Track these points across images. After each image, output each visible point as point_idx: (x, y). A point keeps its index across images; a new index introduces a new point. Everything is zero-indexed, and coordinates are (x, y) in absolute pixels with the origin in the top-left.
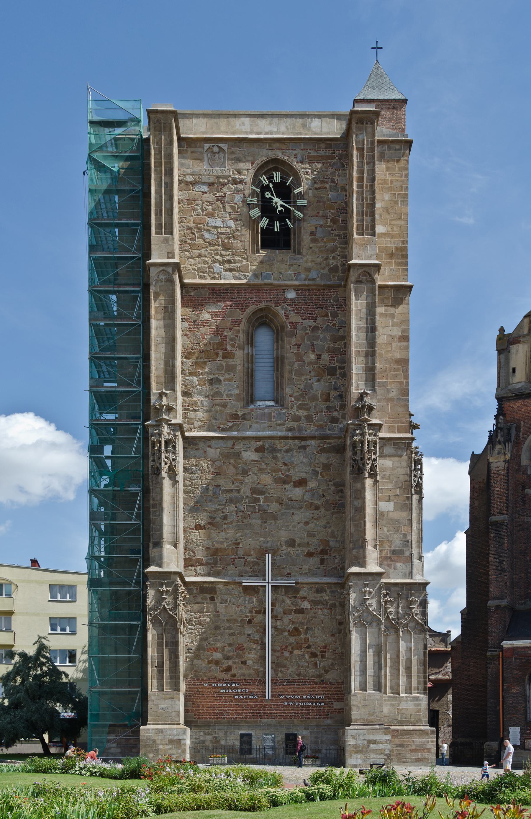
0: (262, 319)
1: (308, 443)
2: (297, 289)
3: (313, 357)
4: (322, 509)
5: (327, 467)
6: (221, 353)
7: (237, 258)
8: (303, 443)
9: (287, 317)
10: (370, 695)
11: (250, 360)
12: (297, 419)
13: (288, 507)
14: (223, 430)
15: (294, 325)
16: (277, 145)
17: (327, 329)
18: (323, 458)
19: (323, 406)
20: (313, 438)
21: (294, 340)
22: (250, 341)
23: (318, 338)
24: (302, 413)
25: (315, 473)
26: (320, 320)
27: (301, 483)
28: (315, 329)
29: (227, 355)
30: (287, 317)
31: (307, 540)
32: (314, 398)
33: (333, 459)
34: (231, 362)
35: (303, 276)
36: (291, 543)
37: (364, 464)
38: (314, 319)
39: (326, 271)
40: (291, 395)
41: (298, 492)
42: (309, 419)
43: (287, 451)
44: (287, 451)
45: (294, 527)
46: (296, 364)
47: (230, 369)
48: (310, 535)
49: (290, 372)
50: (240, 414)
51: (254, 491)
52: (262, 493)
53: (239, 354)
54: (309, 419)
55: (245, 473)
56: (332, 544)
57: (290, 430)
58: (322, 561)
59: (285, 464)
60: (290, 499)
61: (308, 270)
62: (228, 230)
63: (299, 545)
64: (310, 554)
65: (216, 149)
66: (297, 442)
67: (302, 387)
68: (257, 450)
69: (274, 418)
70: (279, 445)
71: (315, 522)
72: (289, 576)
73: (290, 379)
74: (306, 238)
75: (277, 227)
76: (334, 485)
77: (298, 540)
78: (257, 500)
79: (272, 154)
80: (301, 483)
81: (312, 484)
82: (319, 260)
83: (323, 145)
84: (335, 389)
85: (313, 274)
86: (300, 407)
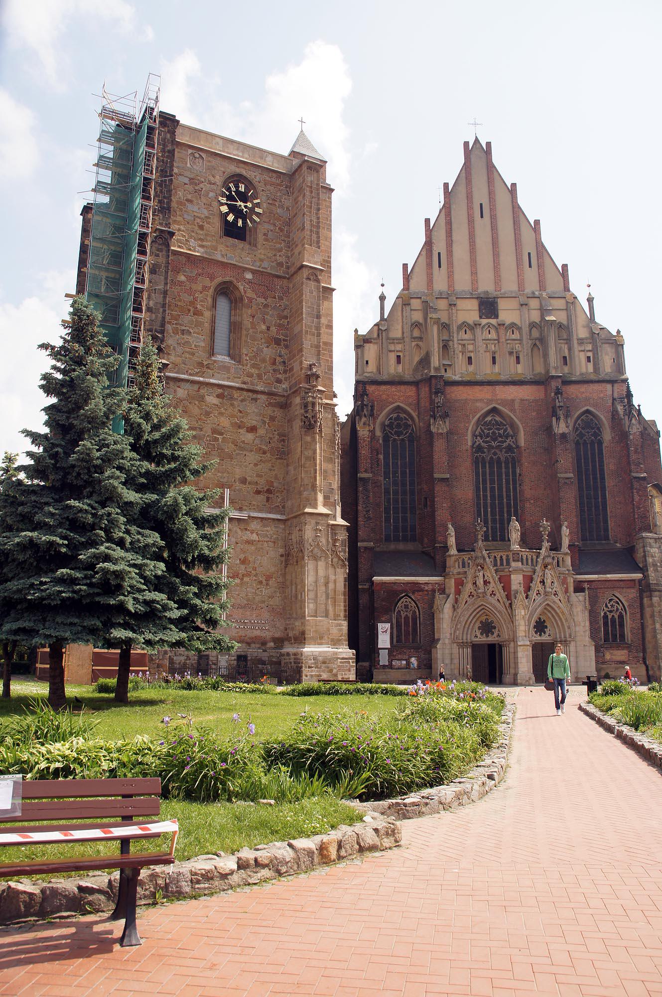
0: (225, 290)
1: (259, 396)
2: (253, 272)
3: (264, 327)
4: (269, 455)
5: (272, 419)
6: (192, 309)
7: (209, 238)
8: (255, 396)
9: (245, 292)
10: (320, 621)
11: (213, 321)
12: (250, 375)
13: (242, 449)
14: (191, 375)
15: (250, 300)
16: (242, 165)
17: (274, 308)
18: (269, 411)
19: (270, 369)
20: (262, 393)
21: (249, 311)
22: (214, 306)
23: (267, 314)
24: (254, 371)
25: (264, 422)
26: (269, 300)
27: (252, 429)
28: (266, 306)
29: (197, 313)
30: (245, 292)
31: (256, 479)
32: (263, 361)
33: (278, 413)
34: (200, 319)
35: (258, 264)
36: (244, 481)
37: (315, 422)
38: (266, 298)
39: (274, 264)
40: (246, 355)
41: (250, 437)
42: (259, 376)
43: (242, 401)
44: (242, 401)
45: (246, 466)
46: (251, 331)
47: (199, 324)
48: (258, 476)
49: (247, 336)
50: (205, 363)
51: (214, 431)
52: (221, 434)
53: (207, 314)
54: (259, 376)
55: (208, 414)
56: (275, 484)
57: (244, 383)
58: (268, 499)
59: (241, 412)
60: (243, 442)
61: (261, 260)
62: (203, 216)
63: (249, 483)
64: (258, 492)
65: (197, 155)
66: (250, 394)
67: (255, 350)
68: (218, 396)
69: (232, 371)
70: (236, 394)
71: (263, 464)
72: (241, 509)
73: (246, 341)
74: (261, 237)
75: (240, 223)
76: (278, 434)
77: (249, 479)
78: (216, 439)
79: (238, 171)
80: (252, 429)
81: (261, 432)
82: (270, 255)
83: (274, 175)
84: (280, 356)
85: (266, 264)
86: (253, 366)
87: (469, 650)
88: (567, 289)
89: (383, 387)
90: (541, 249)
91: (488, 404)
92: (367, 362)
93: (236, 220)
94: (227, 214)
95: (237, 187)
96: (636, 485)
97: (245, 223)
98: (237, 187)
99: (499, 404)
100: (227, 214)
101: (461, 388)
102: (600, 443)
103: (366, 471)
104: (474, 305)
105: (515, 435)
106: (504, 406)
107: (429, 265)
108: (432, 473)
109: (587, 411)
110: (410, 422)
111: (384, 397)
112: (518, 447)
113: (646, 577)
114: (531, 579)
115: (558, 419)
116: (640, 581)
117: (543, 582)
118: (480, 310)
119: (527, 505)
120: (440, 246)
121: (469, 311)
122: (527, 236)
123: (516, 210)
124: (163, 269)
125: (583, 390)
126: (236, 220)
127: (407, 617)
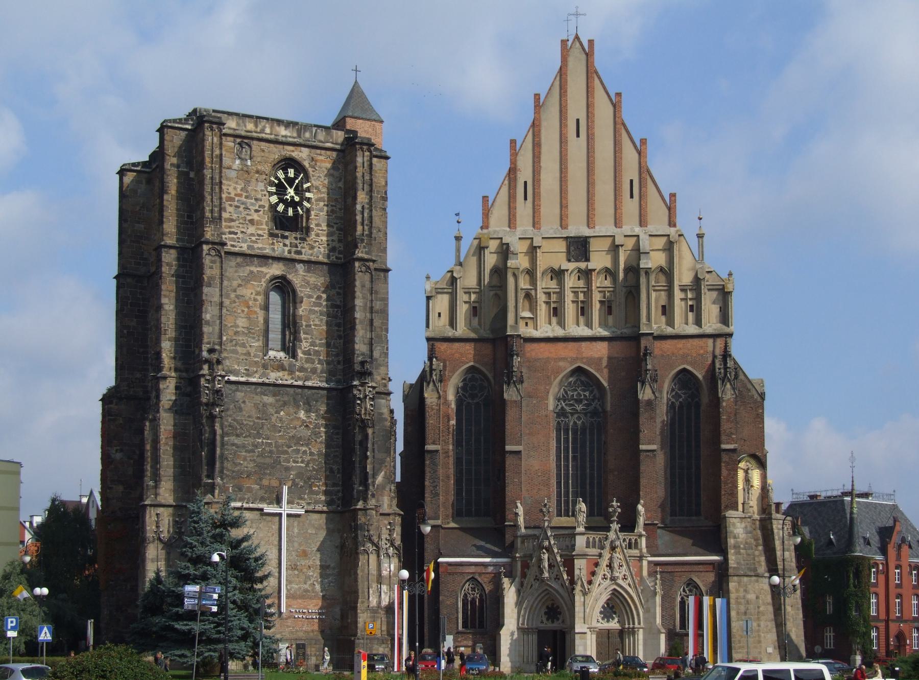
75: (290, 212)
87: (535, 637)
88: (672, 224)
89: (457, 345)
90: (644, 171)
91: (571, 363)
92: (439, 314)
93: (286, 210)
94: (277, 204)
95: (286, 173)
96: (725, 458)
97: (295, 211)
98: (286, 173)
99: (584, 363)
100: (277, 204)
101: (543, 345)
102: (698, 405)
103: (434, 443)
104: (562, 246)
106: (589, 365)
107: (512, 197)
109: (684, 370)
110: (486, 384)
111: (457, 356)
112: (604, 411)
113: (726, 560)
114: (597, 565)
115: (643, 383)
117: (610, 566)
118: (568, 252)
120: (525, 174)
121: (554, 255)
122: (630, 155)
123: (619, 125)
124: (218, 281)
125: (680, 346)
126: (286, 210)
127: (473, 600)
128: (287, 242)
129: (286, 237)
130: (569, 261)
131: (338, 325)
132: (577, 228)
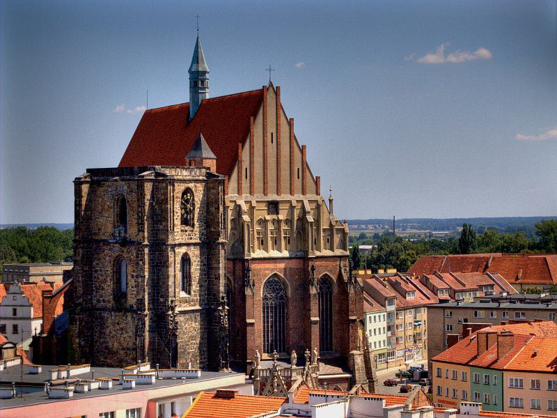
88: (318, 193)
102: (331, 293)
104: (263, 206)
105: (286, 288)
108: (245, 319)
109: (326, 274)
112: (286, 296)
113: (354, 376)
116: (351, 378)
119: (291, 332)
123: (292, 137)
128: (187, 233)
129: (186, 231)
130: (269, 214)
131: (205, 275)
132: (273, 197)
